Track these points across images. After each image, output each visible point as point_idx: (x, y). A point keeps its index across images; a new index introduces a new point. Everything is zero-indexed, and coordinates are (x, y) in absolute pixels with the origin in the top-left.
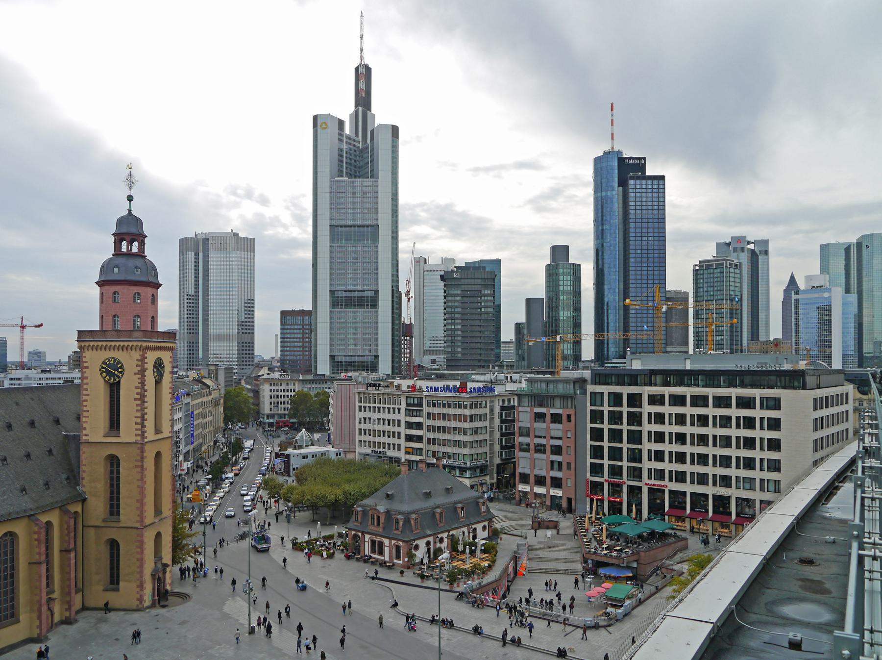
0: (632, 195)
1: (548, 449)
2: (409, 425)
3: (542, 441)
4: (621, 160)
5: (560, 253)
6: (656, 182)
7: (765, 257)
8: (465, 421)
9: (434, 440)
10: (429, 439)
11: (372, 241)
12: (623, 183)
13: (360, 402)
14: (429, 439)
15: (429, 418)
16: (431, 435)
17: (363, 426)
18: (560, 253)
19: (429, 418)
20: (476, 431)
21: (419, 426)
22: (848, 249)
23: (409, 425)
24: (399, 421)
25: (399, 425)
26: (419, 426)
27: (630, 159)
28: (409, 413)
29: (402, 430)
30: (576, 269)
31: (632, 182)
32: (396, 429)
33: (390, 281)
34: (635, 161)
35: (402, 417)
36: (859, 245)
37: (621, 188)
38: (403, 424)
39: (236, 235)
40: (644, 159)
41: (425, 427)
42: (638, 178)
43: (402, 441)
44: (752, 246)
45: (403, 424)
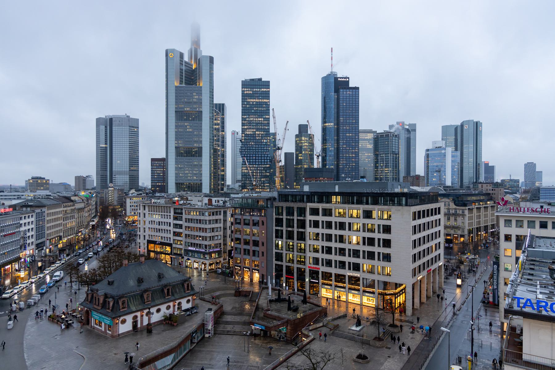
0: (341, 97)
1: (251, 243)
2: (176, 226)
3: (248, 238)
4: (336, 79)
5: (303, 129)
6: (354, 90)
7: (414, 132)
8: (206, 223)
9: (189, 235)
10: (186, 235)
11: (199, 121)
12: (337, 91)
13: (149, 211)
14: (186, 235)
15: (186, 222)
16: (187, 232)
17: (150, 226)
18: (303, 129)
19: (186, 222)
20: (213, 230)
21: (181, 226)
22: (456, 129)
23: (176, 226)
24: (170, 223)
25: (170, 226)
26: (181, 226)
27: (341, 78)
28: (175, 218)
29: (171, 228)
30: (311, 137)
31: (342, 90)
32: (168, 228)
33: (209, 142)
34: (343, 79)
35: (171, 221)
36: (462, 126)
37: (336, 94)
38: (172, 225)
39: (128, 117)
40: (348, 78)
41: (184, 227)
42: (345, 88)
43: (171, 235)
44: (407, 127)
45: (172, 225)
